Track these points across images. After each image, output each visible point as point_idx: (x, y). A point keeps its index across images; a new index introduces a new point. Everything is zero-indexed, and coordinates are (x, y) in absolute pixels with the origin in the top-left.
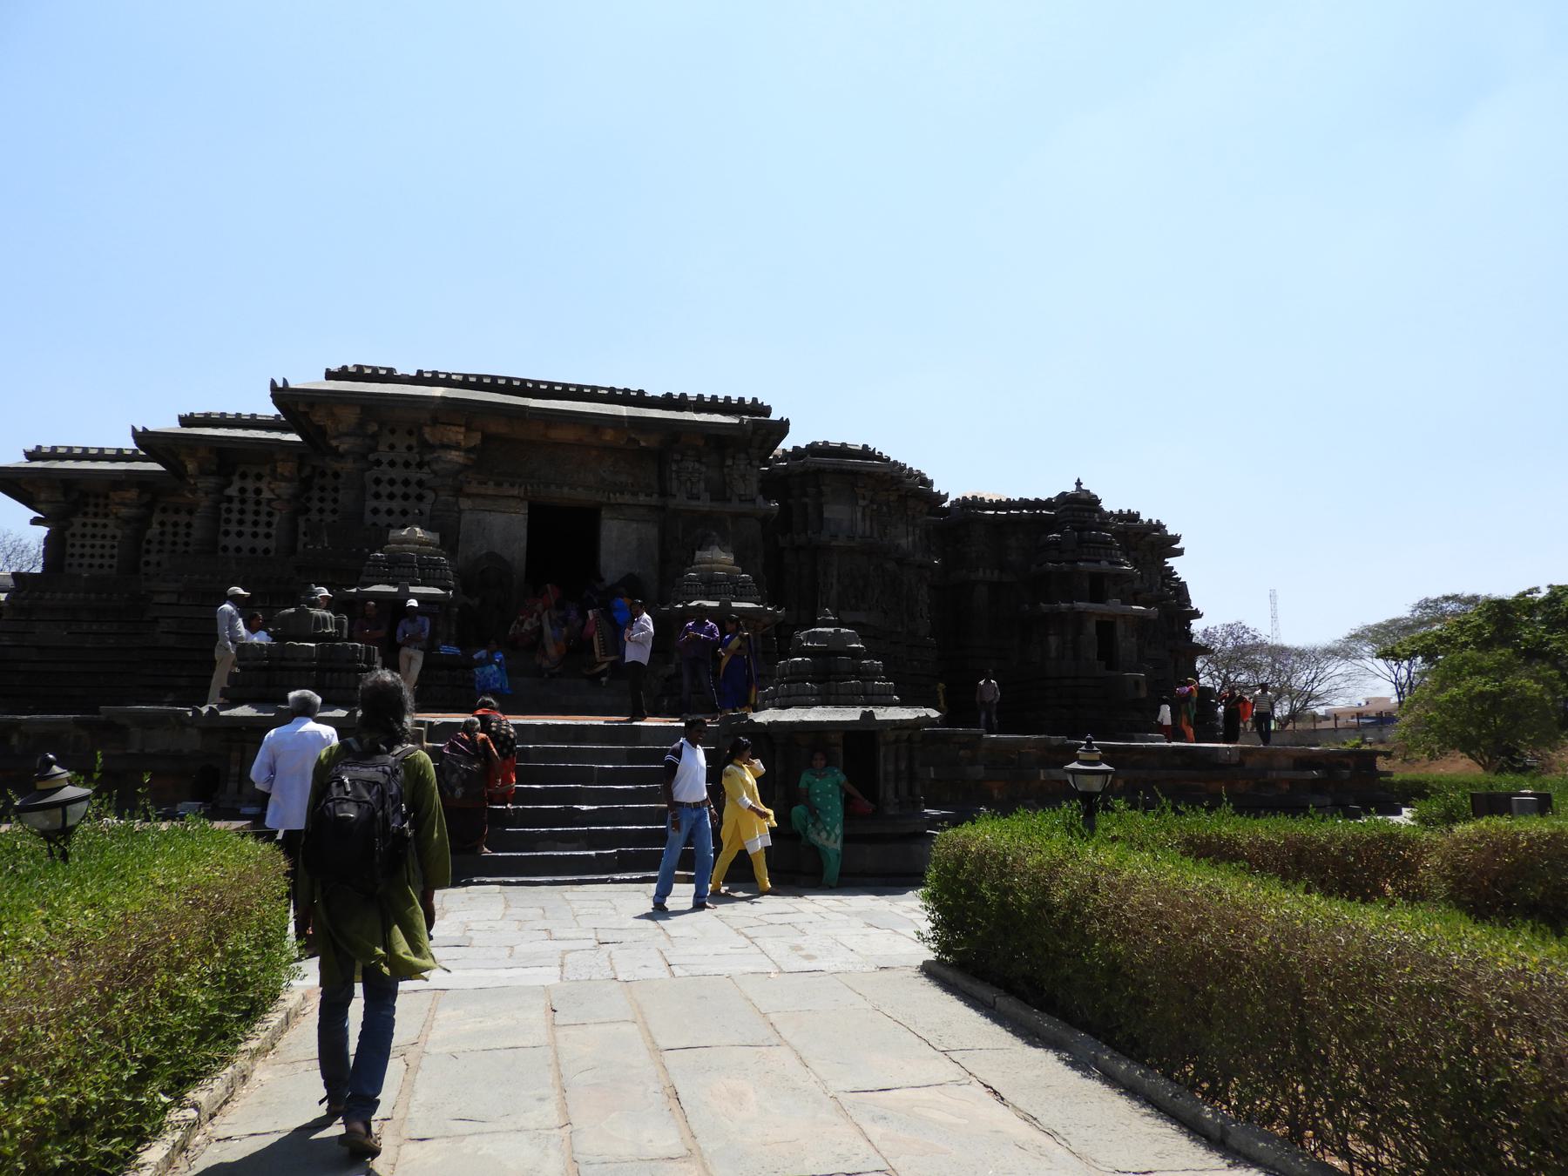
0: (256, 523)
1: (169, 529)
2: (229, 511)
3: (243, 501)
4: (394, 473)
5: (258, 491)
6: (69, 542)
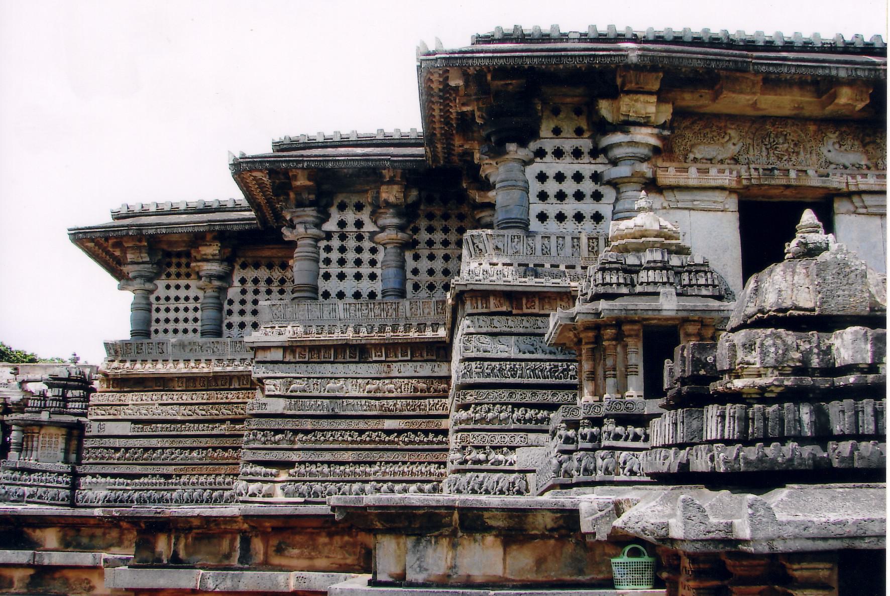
0: (358, 262)
1: (250, 286)
2: (328, 249)
3: (343, 237)
4: (567, 166)
5: (359, 224)
6: (154, 307)
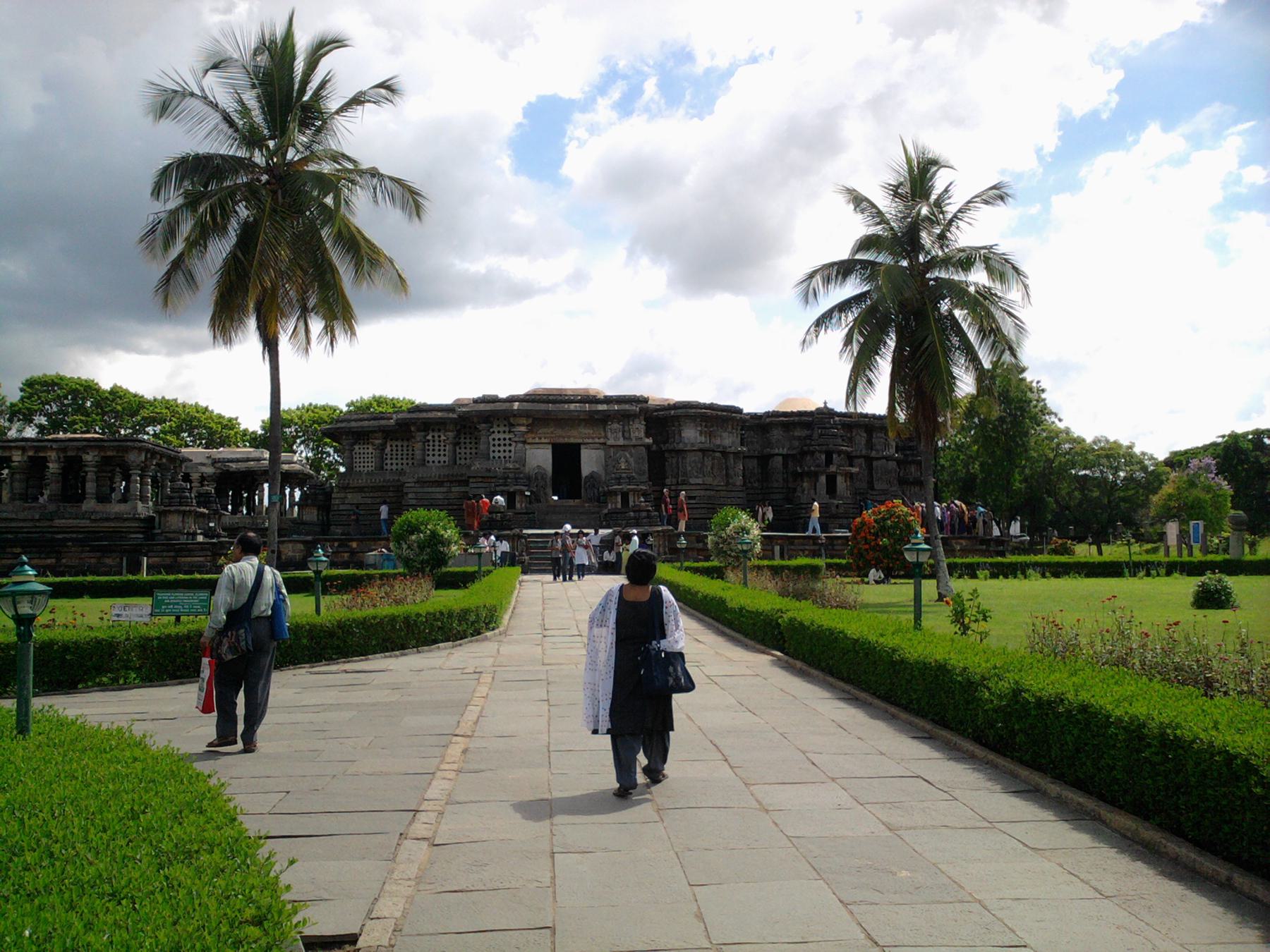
0: (439, 450)
1: (394, 448)
2: (429, 446)
3: (434, 441)
4: (502, 436)
5: (439, 437)
